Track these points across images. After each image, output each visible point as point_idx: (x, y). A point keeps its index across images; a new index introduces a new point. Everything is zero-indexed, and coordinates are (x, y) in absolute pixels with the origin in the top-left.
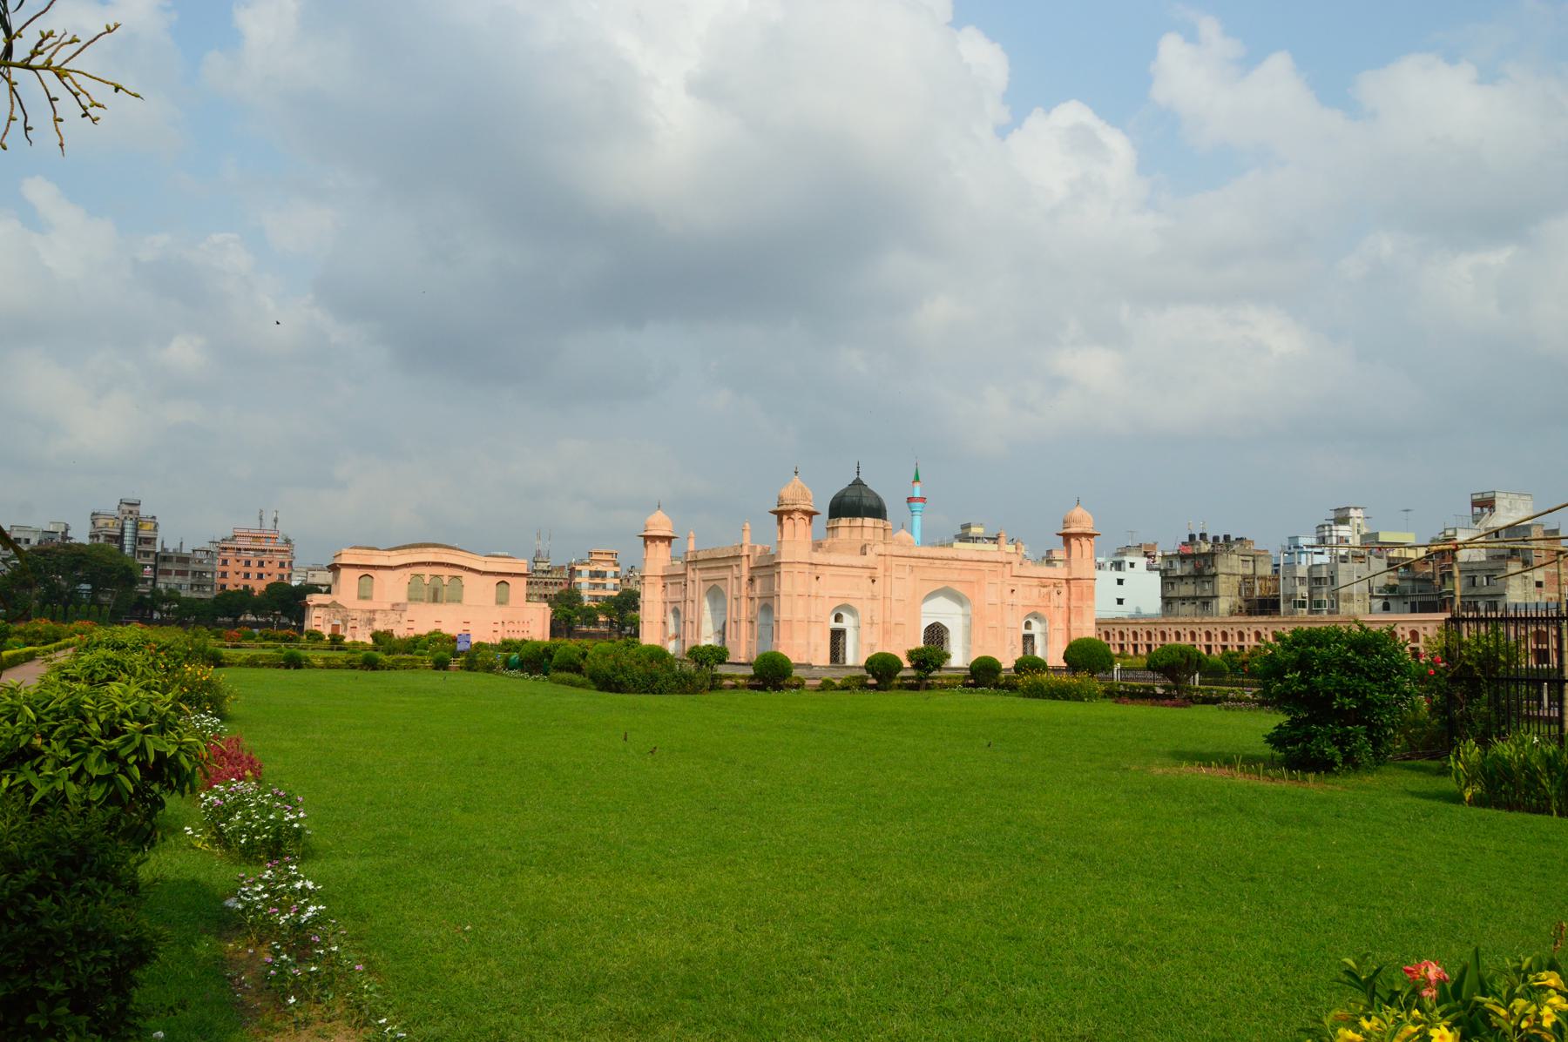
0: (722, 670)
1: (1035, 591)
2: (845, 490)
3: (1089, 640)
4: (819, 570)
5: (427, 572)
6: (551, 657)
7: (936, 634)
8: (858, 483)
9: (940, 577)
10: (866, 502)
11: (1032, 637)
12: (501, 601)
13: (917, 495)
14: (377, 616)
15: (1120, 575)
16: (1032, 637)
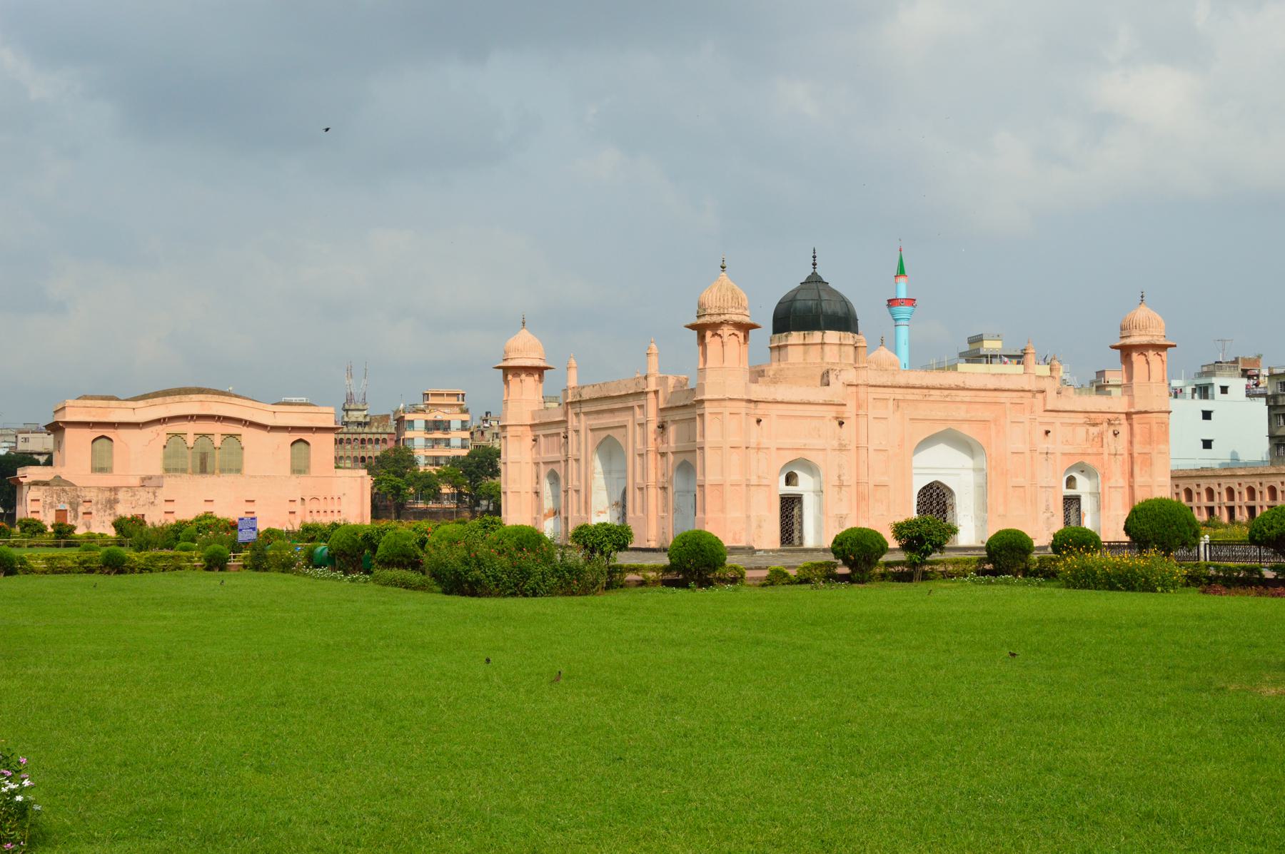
0: (622, 559)
1: (1081, 431)
2: (797, 290)
3: (1162, 502)
4: (761, 410)
5: (190, 428)
6: (374, 548)
7: (935, 498)
8: (814, 280)
9: (940, 415)
10: (829, 307)
11: (1077, 499)
12: (299, 469)
13: (902, 294)
14: (121, 495)
15: (1207, 405)
16: (1077, 499)
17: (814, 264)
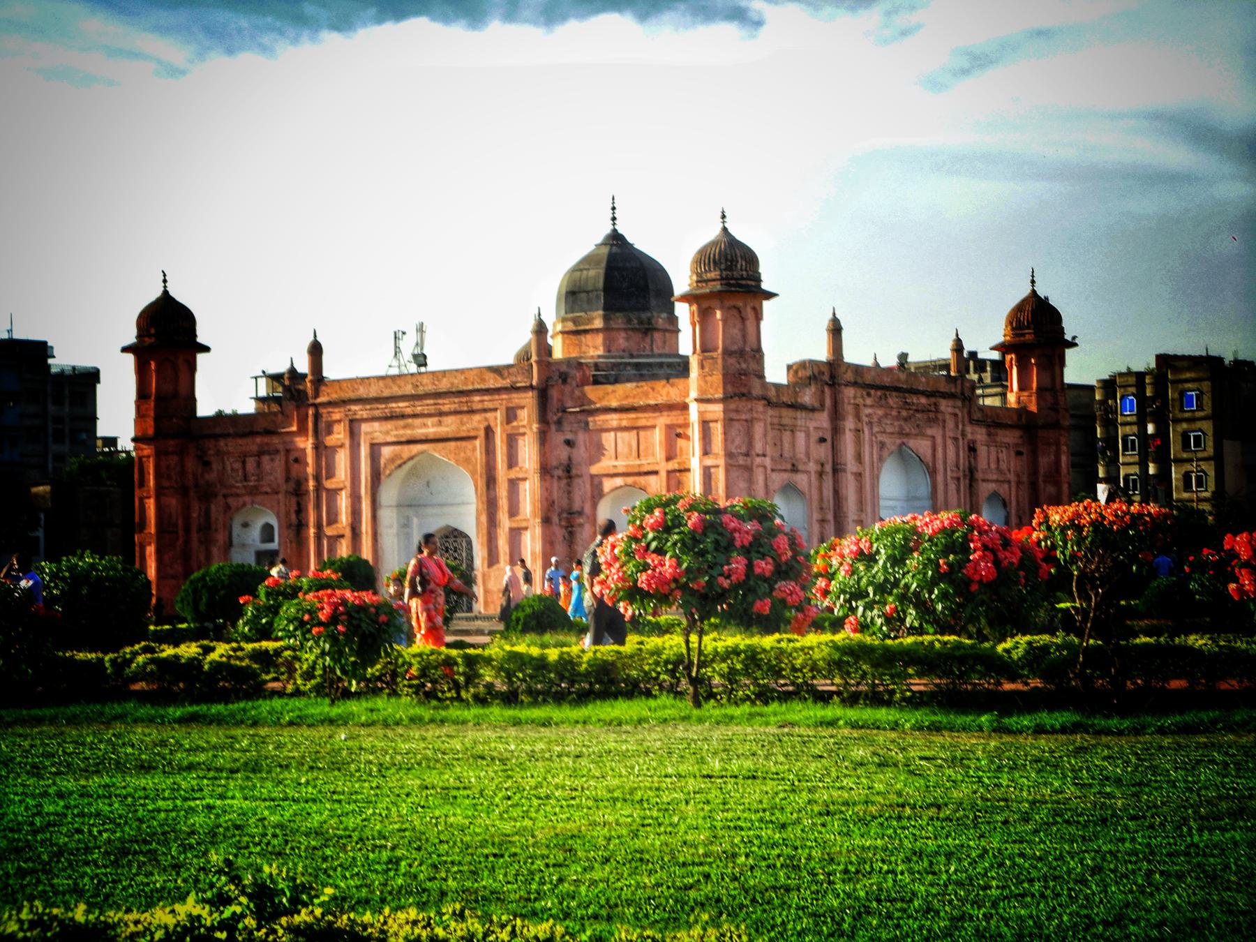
8: (616, 238)
17: (614, 219)
